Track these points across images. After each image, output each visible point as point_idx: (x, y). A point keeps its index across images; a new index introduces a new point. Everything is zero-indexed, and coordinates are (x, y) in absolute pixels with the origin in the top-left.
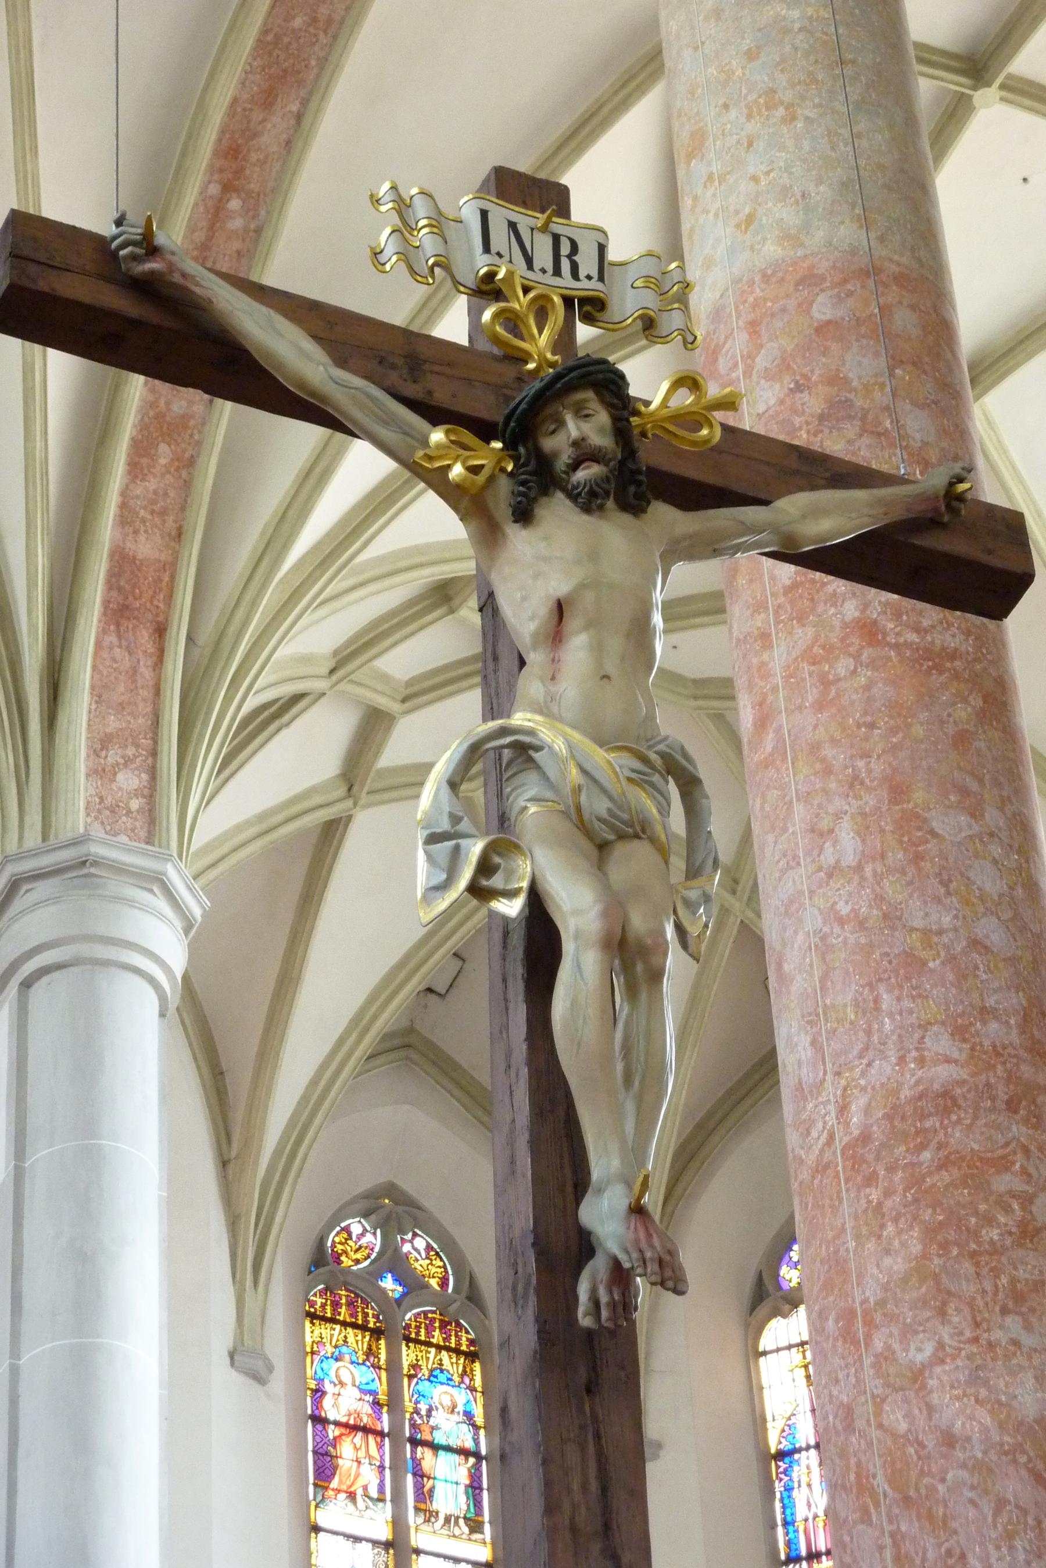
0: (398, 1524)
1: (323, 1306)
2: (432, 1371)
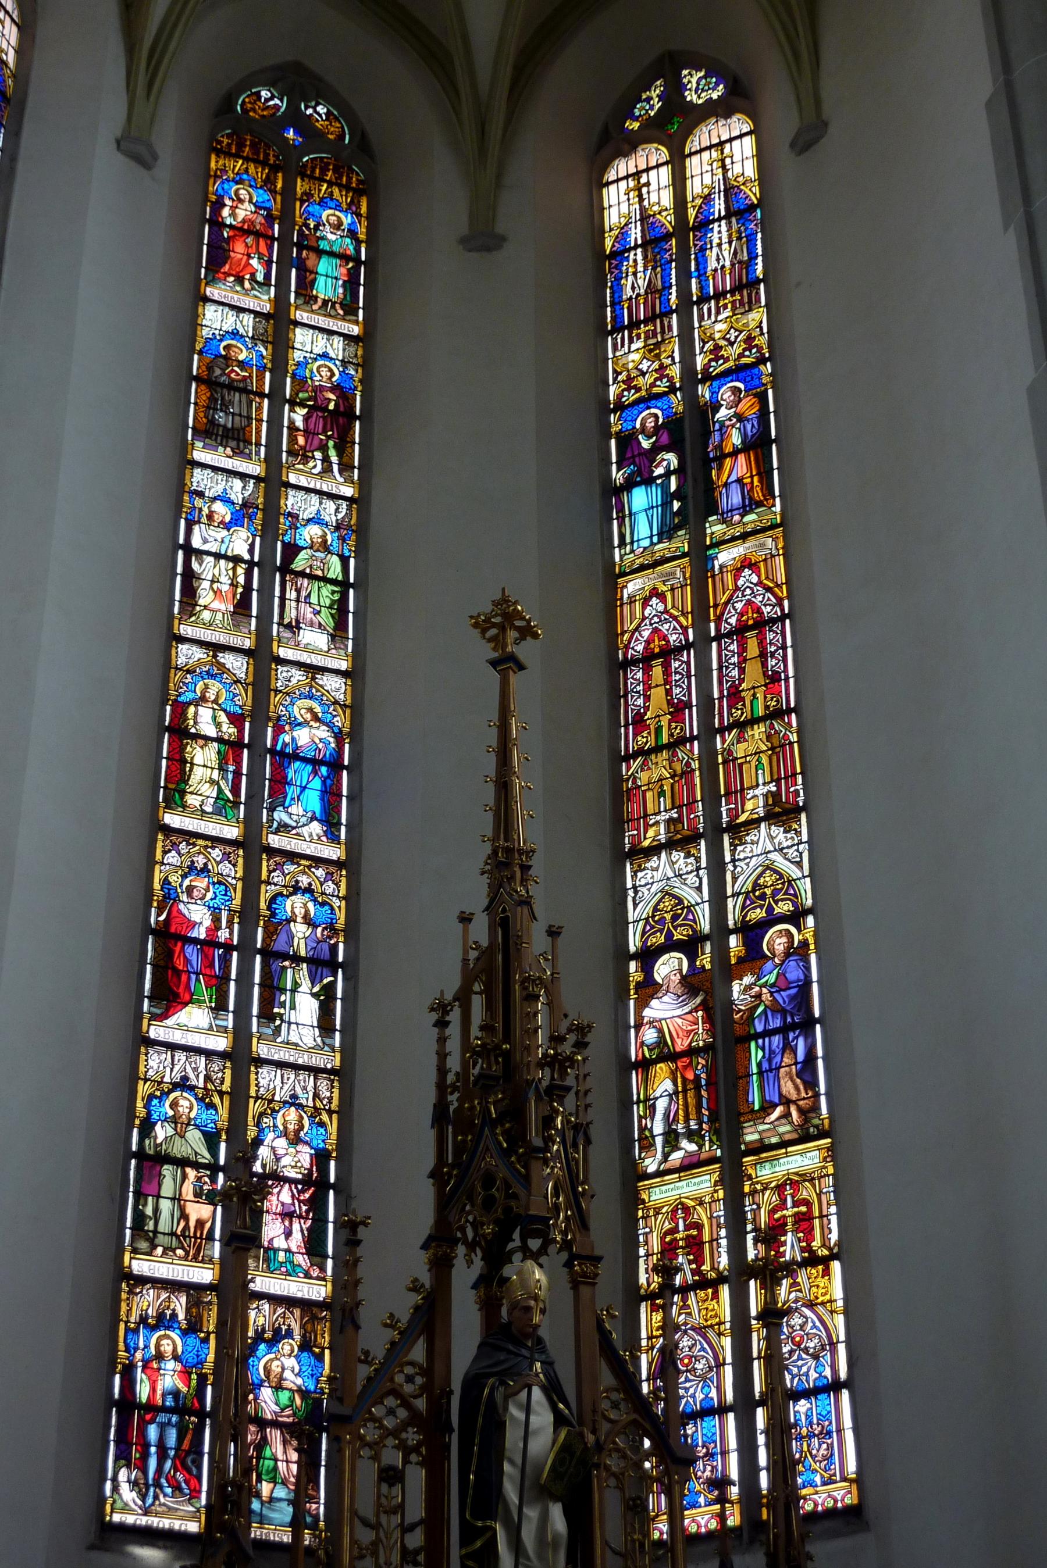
0: (280, 302)
1: (229, 145)
2: (323, 198)
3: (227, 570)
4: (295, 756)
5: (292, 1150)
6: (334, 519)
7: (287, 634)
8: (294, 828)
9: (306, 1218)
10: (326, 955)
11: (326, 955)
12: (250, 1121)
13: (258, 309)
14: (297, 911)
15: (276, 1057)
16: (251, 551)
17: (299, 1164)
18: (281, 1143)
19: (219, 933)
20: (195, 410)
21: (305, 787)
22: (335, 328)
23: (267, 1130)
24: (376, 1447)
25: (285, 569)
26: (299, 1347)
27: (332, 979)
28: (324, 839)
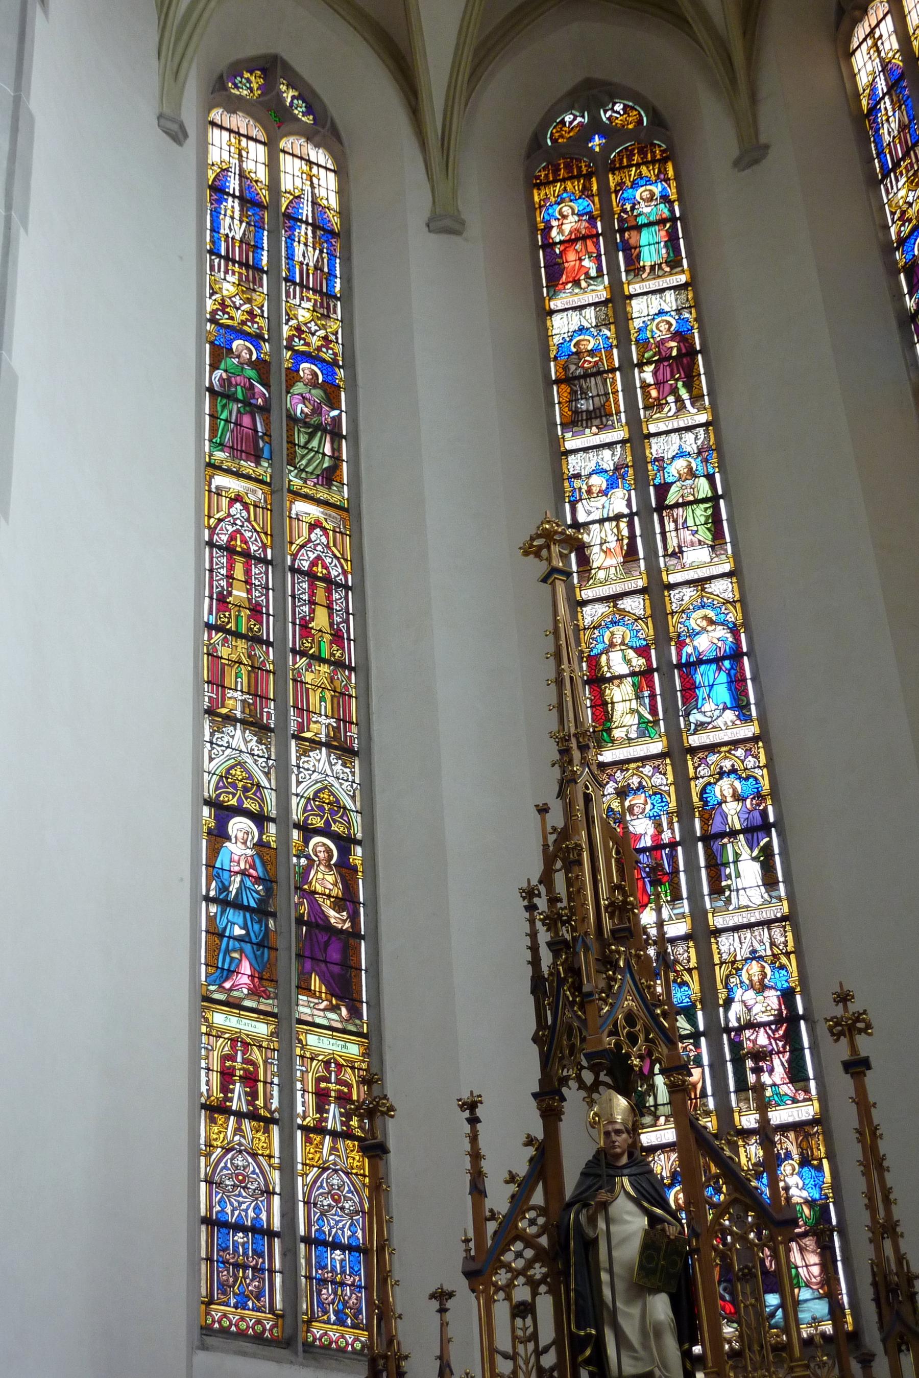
0: (616, 286)
1: (547, 176)
2: (634, 180)
3: (612, 530)
4: (700, 662)
5: (760, 998)
6: (695, 447)
7: (674, 561)
8: (709, 723)
9: (785, 1052)
10: (758, 820)
11: (758, 820)
12: (720, 986)
13: (597, 300)
14: (725, 793)
15: (731, 924)
16: (629, 505)
17: (769, 1008)
18: (750, 996)
19: (663, 836)
20: (560, 408)
21: (713, 685)
22: (665, 286)
23: (735, 989)
24: (508, 1288)
25: (661, 507)
26: (799, 1164)
27: (767, 839)
28: (738, 722)
